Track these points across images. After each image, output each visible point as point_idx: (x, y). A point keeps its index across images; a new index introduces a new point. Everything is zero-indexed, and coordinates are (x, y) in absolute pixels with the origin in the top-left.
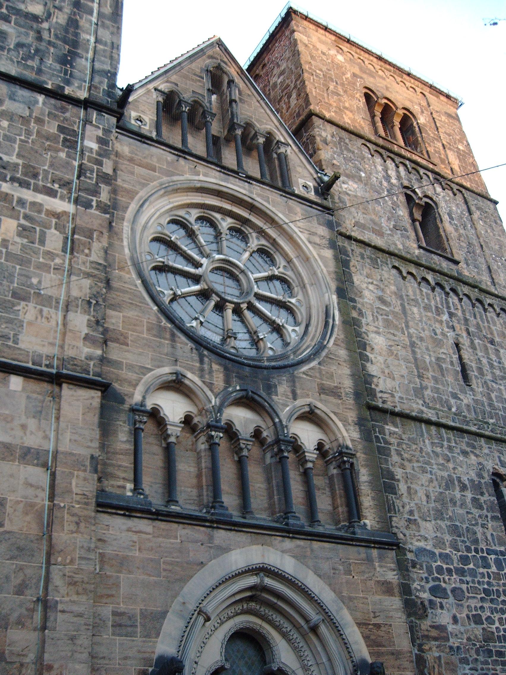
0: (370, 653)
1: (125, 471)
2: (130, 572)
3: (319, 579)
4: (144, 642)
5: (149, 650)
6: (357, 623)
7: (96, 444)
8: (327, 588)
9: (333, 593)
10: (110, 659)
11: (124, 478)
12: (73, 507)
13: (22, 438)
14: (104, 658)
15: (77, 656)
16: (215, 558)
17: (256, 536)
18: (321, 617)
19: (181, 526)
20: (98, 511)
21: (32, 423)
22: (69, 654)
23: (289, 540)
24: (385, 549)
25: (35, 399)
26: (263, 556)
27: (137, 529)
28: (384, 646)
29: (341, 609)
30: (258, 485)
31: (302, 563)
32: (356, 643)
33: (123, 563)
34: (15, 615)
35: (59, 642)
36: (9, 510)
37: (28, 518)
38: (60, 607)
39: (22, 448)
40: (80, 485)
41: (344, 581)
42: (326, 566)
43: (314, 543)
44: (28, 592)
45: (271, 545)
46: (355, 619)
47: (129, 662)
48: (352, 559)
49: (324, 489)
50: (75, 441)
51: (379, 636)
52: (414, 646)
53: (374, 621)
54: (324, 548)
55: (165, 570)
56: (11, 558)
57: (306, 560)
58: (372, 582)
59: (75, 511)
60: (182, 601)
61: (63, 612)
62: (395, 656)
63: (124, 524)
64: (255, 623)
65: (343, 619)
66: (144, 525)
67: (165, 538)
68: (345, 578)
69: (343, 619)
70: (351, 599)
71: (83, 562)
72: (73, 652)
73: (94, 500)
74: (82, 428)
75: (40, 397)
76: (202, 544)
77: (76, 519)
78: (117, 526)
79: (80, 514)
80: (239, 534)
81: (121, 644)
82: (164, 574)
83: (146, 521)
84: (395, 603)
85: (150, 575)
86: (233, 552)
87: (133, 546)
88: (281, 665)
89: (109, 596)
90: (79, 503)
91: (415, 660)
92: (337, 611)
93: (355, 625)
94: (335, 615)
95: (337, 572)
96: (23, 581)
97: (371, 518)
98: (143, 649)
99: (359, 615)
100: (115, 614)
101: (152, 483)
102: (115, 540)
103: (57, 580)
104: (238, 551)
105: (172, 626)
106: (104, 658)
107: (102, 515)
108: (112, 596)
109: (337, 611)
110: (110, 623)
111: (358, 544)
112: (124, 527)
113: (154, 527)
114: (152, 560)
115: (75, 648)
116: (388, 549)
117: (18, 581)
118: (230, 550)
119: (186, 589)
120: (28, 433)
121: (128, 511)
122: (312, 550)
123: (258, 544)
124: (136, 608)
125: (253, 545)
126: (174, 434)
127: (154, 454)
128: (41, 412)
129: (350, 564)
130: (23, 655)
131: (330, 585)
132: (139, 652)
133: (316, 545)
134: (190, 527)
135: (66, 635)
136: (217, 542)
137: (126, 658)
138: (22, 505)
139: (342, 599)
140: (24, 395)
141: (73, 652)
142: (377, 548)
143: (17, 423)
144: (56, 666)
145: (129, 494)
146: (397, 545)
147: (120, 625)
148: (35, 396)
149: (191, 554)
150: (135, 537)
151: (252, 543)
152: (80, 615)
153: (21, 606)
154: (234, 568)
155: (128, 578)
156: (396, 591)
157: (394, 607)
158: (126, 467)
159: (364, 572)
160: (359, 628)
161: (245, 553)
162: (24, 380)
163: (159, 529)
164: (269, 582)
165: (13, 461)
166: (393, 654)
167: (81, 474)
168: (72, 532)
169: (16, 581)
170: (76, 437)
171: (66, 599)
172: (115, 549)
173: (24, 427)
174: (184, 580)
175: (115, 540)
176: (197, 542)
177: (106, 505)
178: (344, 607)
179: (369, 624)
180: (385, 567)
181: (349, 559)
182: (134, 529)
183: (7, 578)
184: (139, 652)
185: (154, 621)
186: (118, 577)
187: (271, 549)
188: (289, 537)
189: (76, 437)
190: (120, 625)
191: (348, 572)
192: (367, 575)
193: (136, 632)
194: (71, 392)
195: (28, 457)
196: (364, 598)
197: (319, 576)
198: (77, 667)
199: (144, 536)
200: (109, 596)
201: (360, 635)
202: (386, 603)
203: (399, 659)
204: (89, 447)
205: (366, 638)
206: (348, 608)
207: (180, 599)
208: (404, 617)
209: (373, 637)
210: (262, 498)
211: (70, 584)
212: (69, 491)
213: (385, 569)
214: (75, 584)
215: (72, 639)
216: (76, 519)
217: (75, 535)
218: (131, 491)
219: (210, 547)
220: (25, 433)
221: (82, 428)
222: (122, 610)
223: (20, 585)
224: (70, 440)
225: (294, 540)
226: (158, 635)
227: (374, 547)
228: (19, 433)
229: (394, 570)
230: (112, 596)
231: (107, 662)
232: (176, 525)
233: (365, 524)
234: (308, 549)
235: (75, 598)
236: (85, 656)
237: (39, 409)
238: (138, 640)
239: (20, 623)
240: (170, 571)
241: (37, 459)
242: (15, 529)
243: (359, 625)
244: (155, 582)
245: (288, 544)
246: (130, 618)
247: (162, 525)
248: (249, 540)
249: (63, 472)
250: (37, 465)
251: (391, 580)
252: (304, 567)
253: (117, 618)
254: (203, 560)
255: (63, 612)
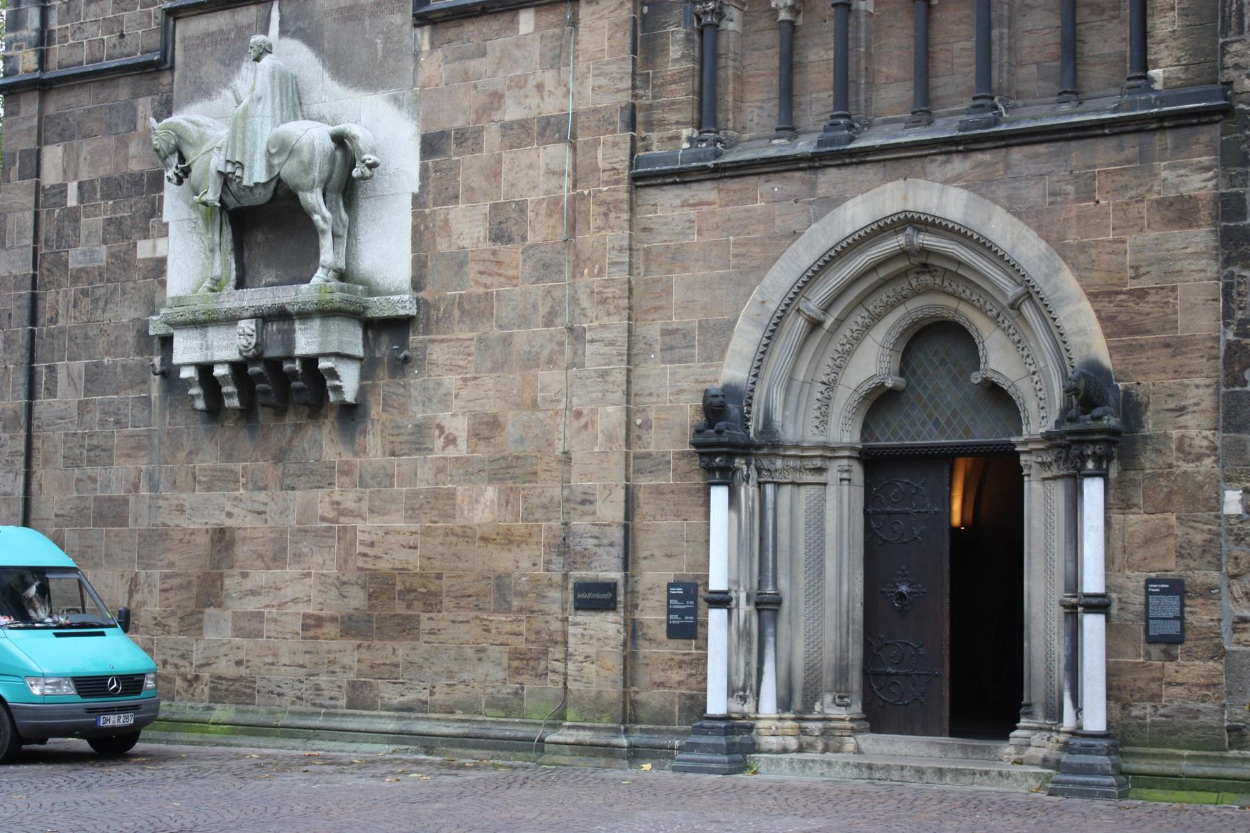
0: (1109, 348)
1: (680, 110)
2: (685, 269)
3: (1015, 220)
4: (703, 367)
5: (709, 378)
6: (1089, 295)
7: (628, 83)
8: (1032, 235)
9: (1043, 242)
10: (658, 396)
11: (677, 123)
12: (600, 191)
13: (539, 107)
14: (651, 394)
15: (609, 396)
16: (816, 220)
17: (895, 164)
18: (1020, 290)
19: (763, 178)
20: (637, 187)
21: (549, 77)
22: (600, 395)
23: (961, 155)
24: (1192, 125)
25: (552, 37)
26: (905, 198)
27: (697, 200)
28: (1149, 332)
29: (1059, 270)
30: (962, 45)
31: (982, 195)
32: (1082, 331)
33: (676, 256)
34: (546, 353)
35: (587, 382)
36: (530, 215)
37: (552, 222)
38: (588, 336)
39: (540, 120)
40: (612, 154)
41: (1073, 214)
42: (1034, 193)
43: (1016, 150)
44: (558, 321)
45: (924, 174)
46: (1085, 287)
47: (682, 397)
48: (1101, 165)
49: (1118, 8)
50: (600, 87)
51: (1140, 314)
52: (1226, 325)
53: (1132, 285)
54: (1037, 155)
55: (735, 256)
56: (538, 280)
57: (993, 188)
58: (1145, 205)
59: (602, 196)
60: (760, 299)
61: (592, 341)
62: (1170, 350)
63: (677, 196)
64: (943, 307)
65: (1057, 290)
66: (706, 192)
67: (737, 204)
68: (1074, 209)
69: (1057, 290)
70: (1083, 248)
71: (613, 269)
72: (605, 392)
73: (627, 173)
74: (608, 63)
75: (557, 31)
76: (796, 202)
77: (603, 209)
78: (667, 206)
79: (609, 199)
80: (861, 168)
81: (673, 374)
82: (733, 262)
83: (709, 185)
84: (1201, 237)
85: (713, 268)
86: (849, 204)
87: (689, 228)
88: (990, 375)
89: (656, 309)
90: (606, 183)
91: (1222, 354)
92: (1047, 277)
93: (1084, 297)
94: (1041, 284)
95: (1059, 199)
96: (552, 307)
97: (1168, 61)
98: (701, 379)
99: (1098, 278)
100: (665, 333)
101: (762, 101)
102: (665, 224)
103: (585, 302)
104: (859, 198)
105: (745, 339)
106: (651, 394)
107: (648, 191)
108: (662, 308)
109: (1047, 277)
110: (658, 347)
111: (1116, 130)
112: (678, 202)
113: (720, 190)
114: (716, 244)
115: (606, 387)
116: (1199, 124)
117: (547, 309)
118: (845, 199)
119: (767, 280)
120: (546, 94)
121: (681, 177)
122: (1008, 167)
123: (897, 179)
124: (693, 321)
125: (887, 181)
126: (781, 5)
127: (768, 48)
128: (559, 55)
129: (1094, 178)
130: (557, 401)
131: (1038, 229)
132: (697, 381)
133: (1017, 154)
134: (777, 175)
135: (596, 371)
136: (821, 191)
137: (679, 392)
138: (544, 205)
139: (1062, 250)
140: (537, 37)
141: (605, 392)
142: (1170, 128)
143: (532, 83)
144: (585, 412)
145: (686, 145)
146: (1227, 112)
147: (672, 348)
148: (551, 31)
149: (778, 221)
150: (693, 213)
151: (885, 180)
152: (612, 343)
153: (551, 340)
154: (849, 231)
155: (682, 279)
156: (1204, 214)
157: (1189, 250)
158: (682, 102)
159: (1125, 188)
160: (1092, 302)
161: (866, 202)
162: (537, 12)
163: (729, 191)
164: (926, 240)
165: (530, 144)
166: (1167, 346)
167: (609, 137)
168: (600, 229)
169: (543, 310)
170: (603, 81)
171: (595, 324)
172: (665, 238)
173: (540, 87)
174: (765, 267)
175: (665, 224)
176: (787, 199)
177: (644, 178)
178: (1065, 266)
179: (1121, 293)
180: (1185, 166)
181: (1095, 167)
182: (691, 202)
183: (535, 306)
184: (697, 381)
185: (718, 335)
186: (670, 280)
187: (921, 181)
188: (958, 152)
189: (603, 81)
190: (672, 348)
191: (1087, 194)
192: (1133, 193)
193: (692, 355)
194: (591, 8)
195: (548, 133)
196: (1115, 241)
197: (1018, 215)
198: (610, 409)
199: (705, 208)
200: (656, 309)
201: (1093, 316)
202: (1170, 245)
203: (1182, 353)
204: (618, 91)
205: (1106, 320)
206: (1074, 267)
207: (755, 295)
208: (1213, 268)
209: (1122, 317)
210: (965, 70)
211: (599, 303)
212: (596, 169)
213: (1182, 172)
214: (603, 302)
215: (604, 374)
216: (603, 209)
217: (603, 233)
218: (690, 140)
219: (810, 203)
220: (542, 98)
221: (608, 63)
222: (675, 326)
223: (549, 313)
224: (593, 89)
225: (971, 154)
226: (722, 357)
227: (1162, 129)
228: (534, 100)
229: (1208, 169)
230: (662, 308)
231: (654, 399)
232: (754, 180)
233: (1152, 81)
234: (1000, 166)
235: (605, 321)
236: (619, 395)
237: (557, 51)
238: (696, 366)
239: (551, 362)
240: (743, 255)
241: (559, 131)
242: (539, 239)
243: (1093, 296)
244: (721, 278)
245: (959, 165)
246: (685, 336)
247: (733, 185)
248: (881, 175)
249: (586, 143)
250: (559, 141)
251: (1192, 194)
252: (987, 202)
253: (667, 339)
254: (797, 228)
255: (592, 341)
